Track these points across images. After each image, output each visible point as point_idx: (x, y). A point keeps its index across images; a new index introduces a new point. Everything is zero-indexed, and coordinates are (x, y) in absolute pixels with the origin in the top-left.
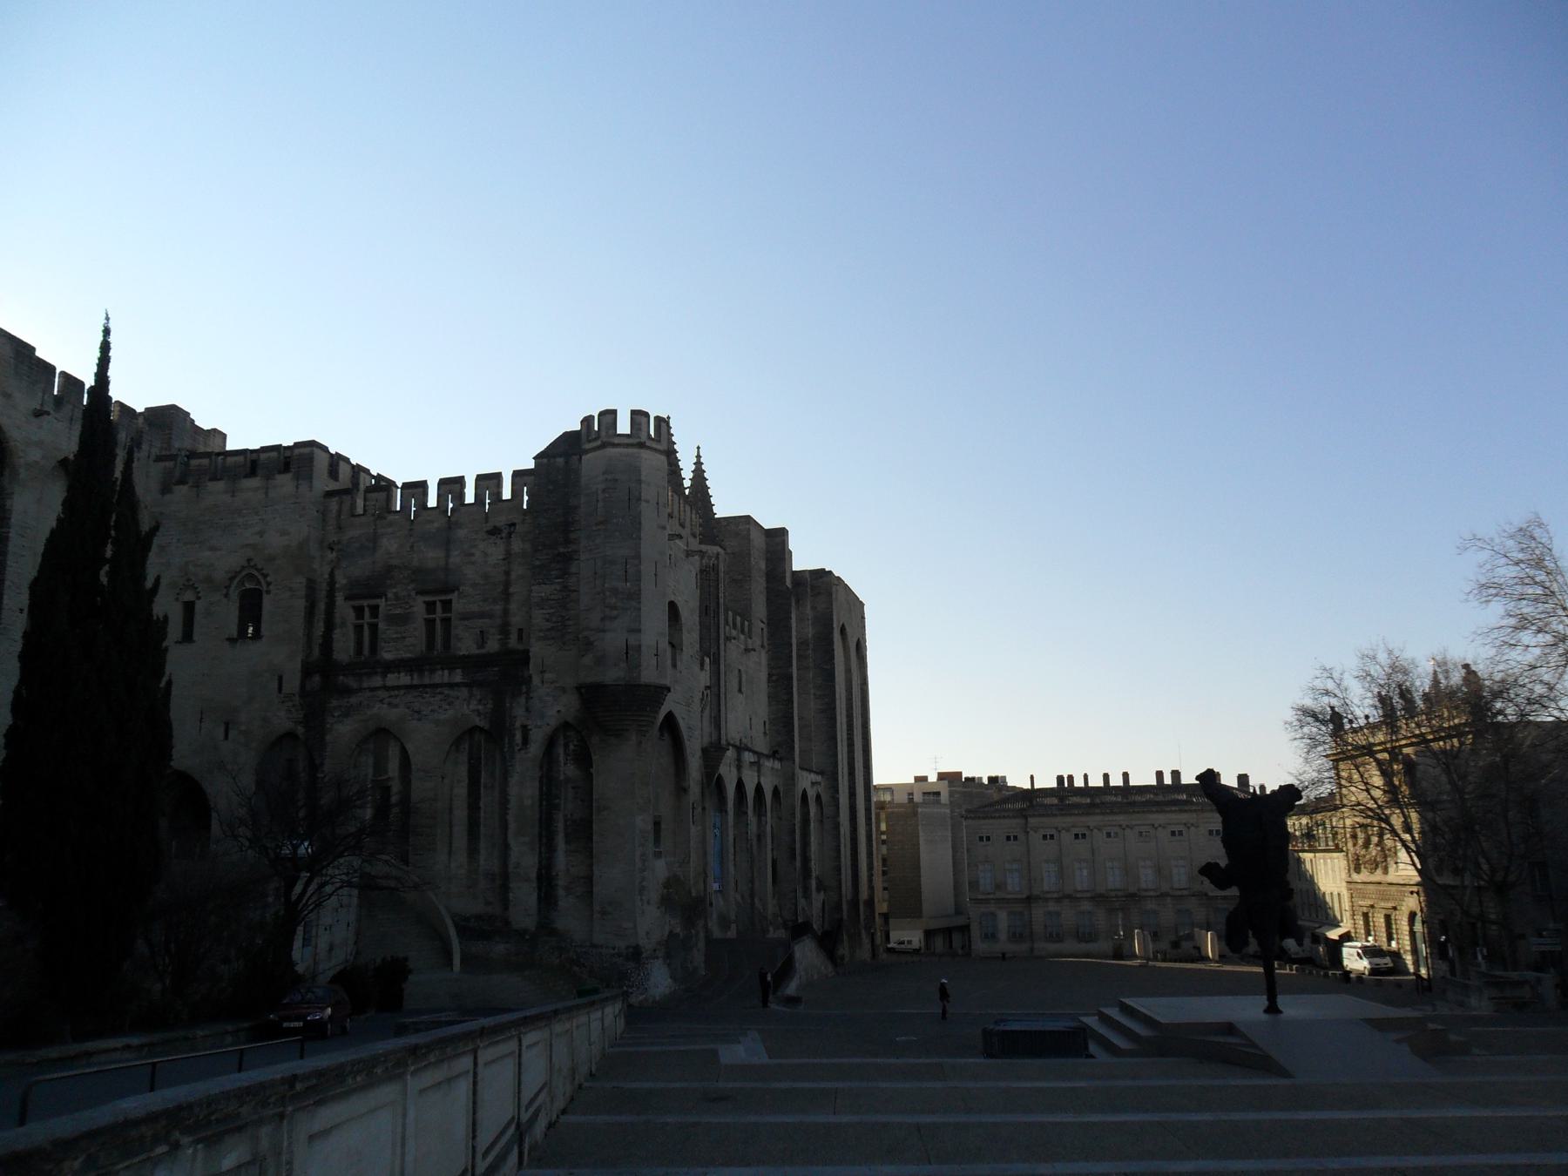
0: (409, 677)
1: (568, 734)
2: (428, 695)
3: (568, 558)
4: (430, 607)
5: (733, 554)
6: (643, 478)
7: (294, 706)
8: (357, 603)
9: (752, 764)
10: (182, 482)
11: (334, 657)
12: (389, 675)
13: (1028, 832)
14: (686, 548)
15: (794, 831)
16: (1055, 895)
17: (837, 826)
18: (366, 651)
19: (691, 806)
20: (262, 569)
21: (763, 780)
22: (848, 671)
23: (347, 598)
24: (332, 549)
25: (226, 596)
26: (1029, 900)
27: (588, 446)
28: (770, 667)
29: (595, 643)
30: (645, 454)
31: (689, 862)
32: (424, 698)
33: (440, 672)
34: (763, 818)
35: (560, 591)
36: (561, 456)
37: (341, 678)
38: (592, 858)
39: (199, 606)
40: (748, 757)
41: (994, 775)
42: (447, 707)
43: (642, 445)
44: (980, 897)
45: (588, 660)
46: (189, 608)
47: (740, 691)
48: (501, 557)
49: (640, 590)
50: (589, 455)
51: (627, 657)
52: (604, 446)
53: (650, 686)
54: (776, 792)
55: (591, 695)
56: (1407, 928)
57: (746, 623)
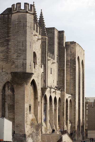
1: (9, 84)
3: (8, 41)
5: (50, 38)
6: (27, 21)
9: (54, 92)
14: (38, 38)
17: (75, 108)
22: (79, 68)
27: (13, 12)
28: (59, 67)
29: (15, 62)
30: (28, 14)
31: (38, 115)
34: (56, 105)
35: (6, 49)
36: (6, 15)
38: (14, 114)
43: (27, 12)
45: (13, 66)
47: (51, 73)
49: (26, 49)
51: (23, 66)
52: (18, 12)
53: (29, 73)
54: (60, 99)
55: (14, 75)
57: (53, 56)
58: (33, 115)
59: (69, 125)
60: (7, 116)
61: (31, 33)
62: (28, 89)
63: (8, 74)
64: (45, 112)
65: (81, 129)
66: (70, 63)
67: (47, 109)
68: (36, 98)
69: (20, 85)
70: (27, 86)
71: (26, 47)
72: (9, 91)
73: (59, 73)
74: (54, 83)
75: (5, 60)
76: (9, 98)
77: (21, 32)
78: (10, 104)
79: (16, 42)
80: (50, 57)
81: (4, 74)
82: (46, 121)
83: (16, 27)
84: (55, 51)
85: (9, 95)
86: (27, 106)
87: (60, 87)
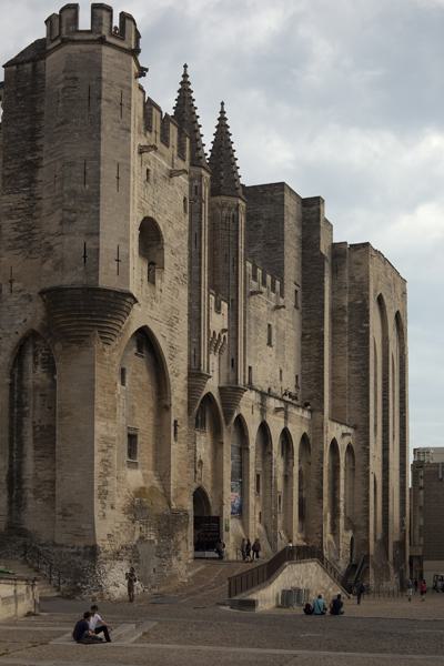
1: (37, 343)
3: (34, 166)
5: (269, 219)
6: (104, 76)
9: (277, 410)
15: (322, 474)
19: (173, 422)
21: (290, 427)
22: (385, 339)
28: (304, 327)
30: (106, 51)
36: (28, 62)
40: (272, 403)
43: (102, 41)
45: (47, 267)
47: (269, 344)
49: (99, 193)
50: (53, 55)
53: (110, 291)
54: (304, 438)
55: (54, 298)
57: (278, 283)
58: (151, 472)
59: (346, 537)
60: (31, 472)
61: (123, 129)
62: (112, 360)
63: (31, 300)
64: (241, 483)
65: (394, 552)
66: (350, 316)
67: (248, 470)
68: (162, 406)
69: (79, 342)
70: (107, 348)
71: (99, 182)
72: (39, 367)
73: (305, 348)
74: (281, 379)
75: (21, 243)
76: (38, 397)
77: (76, 124)
78: (42, 423)
79: (59, 165)
80: (264, 283)
81: (16, 304)
82: (244, 512)
83: (60, 105)
84: (286, 267)
85: (36, 388)
86: (107, 429)
87: (308, 395)
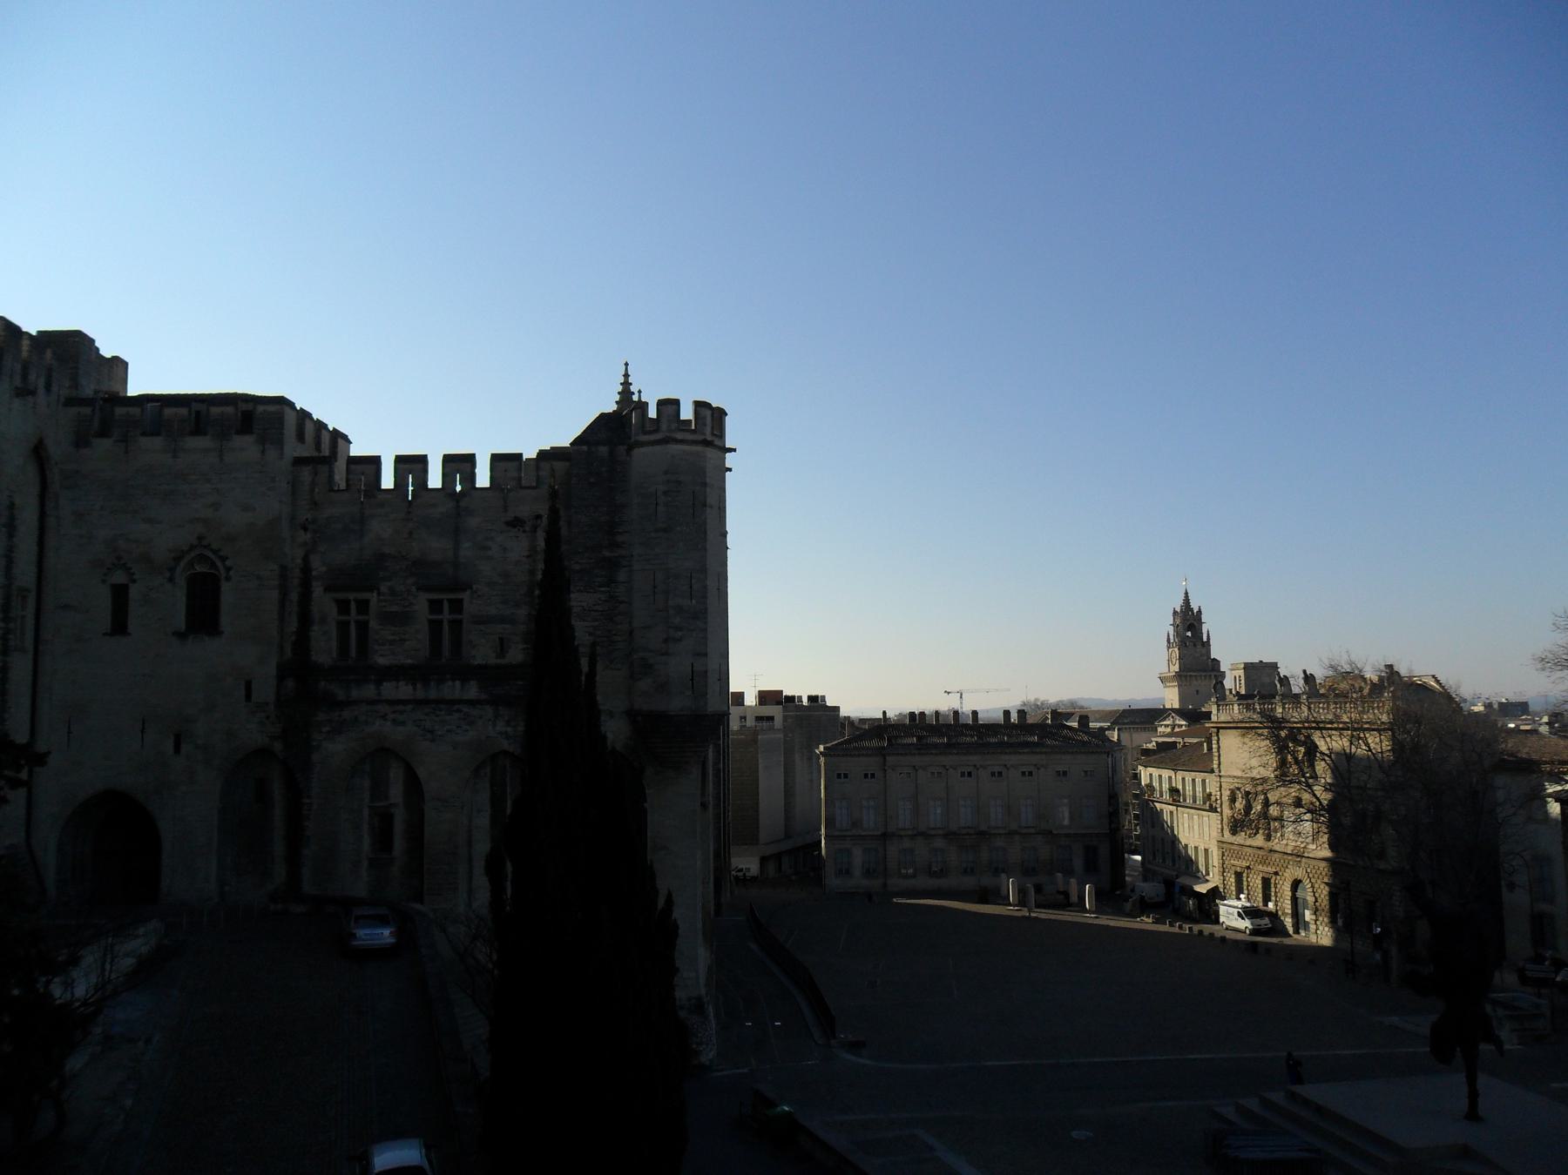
0: (411, 687)
2: (443, 713)
4: (435, 606)
6: (708, 480)
7: (268, 717)
8: (341, 596)
10: (104, 433)
11: (314, 658)
12: (385, 684)
13: (885, 771)
16: (910, 833)
18: (353, 653)
20: (219, 550)
23: (327, 589)
24: (305, 529)
25: (171, 580)
26: (885, 836)
32: (437, 716)
33: (450, 683)
35: (605, 601)
37: (323, 683)
39: (134, 592)
41: (813, 694)
42: (468, 727)
44: (837, 833)
46: (120, 595)
48: (526, 554)
49: (706, 609)
52: (666, 441)
56: (1290, 894)
